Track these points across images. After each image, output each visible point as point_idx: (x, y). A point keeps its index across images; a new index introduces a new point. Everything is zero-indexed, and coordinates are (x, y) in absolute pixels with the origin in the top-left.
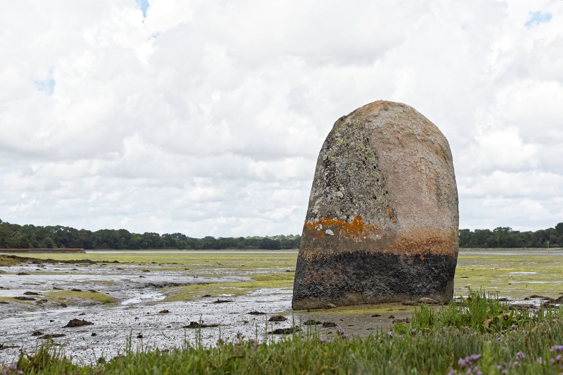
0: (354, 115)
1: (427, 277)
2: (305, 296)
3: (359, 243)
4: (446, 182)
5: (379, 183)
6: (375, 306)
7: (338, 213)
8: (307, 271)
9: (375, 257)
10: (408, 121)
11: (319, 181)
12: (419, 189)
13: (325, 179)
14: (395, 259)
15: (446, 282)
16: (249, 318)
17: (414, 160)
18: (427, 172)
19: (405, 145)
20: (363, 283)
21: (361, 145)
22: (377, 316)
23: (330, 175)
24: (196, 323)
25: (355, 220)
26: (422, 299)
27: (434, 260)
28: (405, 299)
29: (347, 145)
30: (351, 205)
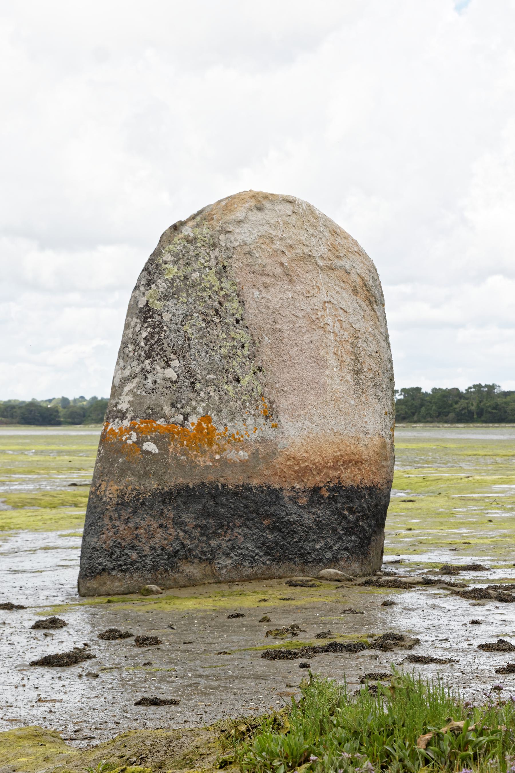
0: (198, 219)
1: (334, 530)
2: (104, 570)
3: (207, 467)
4: (372, 348)
6: (235, 588)
7: (167, 409)
8: (106, 521)
9: (236, 494)
10: (301, 231)
11: (131, 347)
12: (320, 362)
13: (142, 344)
14: (273, 497)
15: (370, 538)
17: (312, 306)
18: (336, 329)
19: (295, 278)
20: (213, 543)
21: (211, 278)
22: (238, 616)
23: (152, 337)
25: (199, 424)
27: (348, 497)
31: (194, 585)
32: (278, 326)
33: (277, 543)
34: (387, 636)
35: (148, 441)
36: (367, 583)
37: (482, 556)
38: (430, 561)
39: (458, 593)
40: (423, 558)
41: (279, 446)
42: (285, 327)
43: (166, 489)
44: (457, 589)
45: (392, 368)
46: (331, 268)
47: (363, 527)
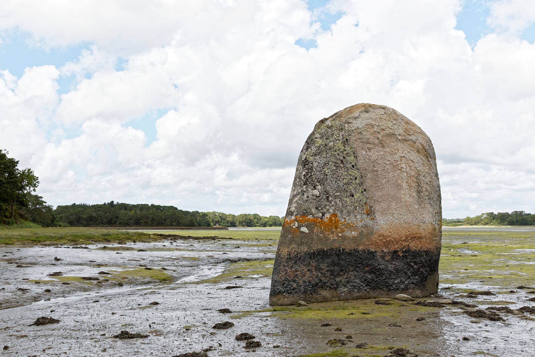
0: (334, 117)
1: (406, 273)
2: (279, 292)
3: (334, 240)
4: (428, 179)
7: (313, 210)
8: (282, 267)
9: (350, 254)
10: (389, 122)
11: (298, 180)
12: (399, 187)
13: (303, 178)
15: (427, 277)
20: (338, 279)
21: (339, 145)
22: (327, 325)
23: (308, 175)
25: (331, 218)
26: (398, 296)
27: (413, 256)
28: (382, 294)
30: (327, 203)
31: (327, 301)
32: (375, 169)
33: (373, 280)
35: (303, 226)
36: (419, 304)
37: (496, 285)
38: (467, 288)
39: (467, 312)
40: (463, 286)
41: (375, 229)
42: (380, 169)
43: (312, 251)
44: (470, 309)
45: (440, 190)
46: (405, 140)
47: (422, 271)
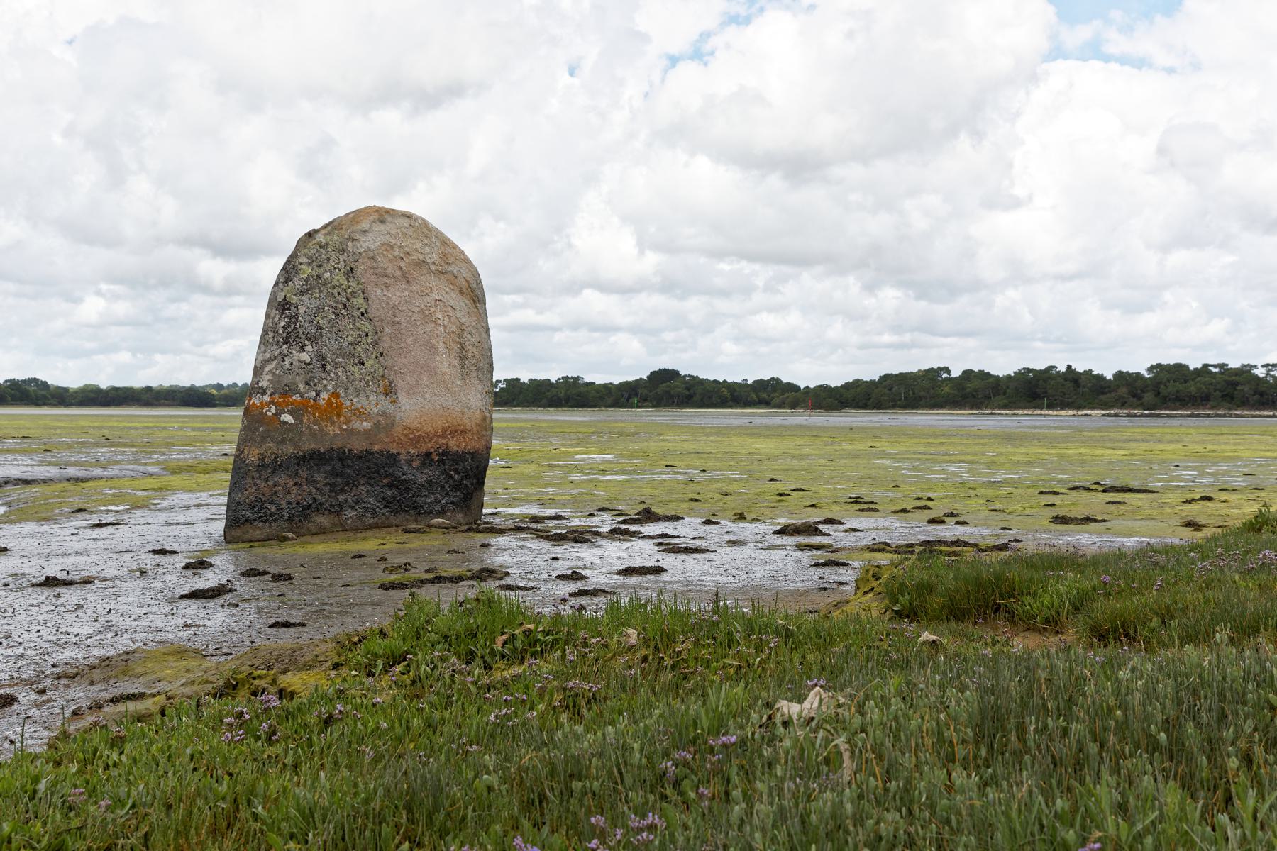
1: (443, 487)
4: (475, 339)
5: (370, 340)
7: (301, 387)
8: (249, 480)
11: (271, 334)
12: (432, 349)
16: (149, 561)
20: (341, 498)
21: (340, 278)
22: (360, 556)
24: (55, 579)
26: (434, 521)
28: (407, 521)
29: (318, 277)
33: (394, 498)
34: (482, 570)
36: (469, 530)
40: (516, 511)
46: (442, 273)
